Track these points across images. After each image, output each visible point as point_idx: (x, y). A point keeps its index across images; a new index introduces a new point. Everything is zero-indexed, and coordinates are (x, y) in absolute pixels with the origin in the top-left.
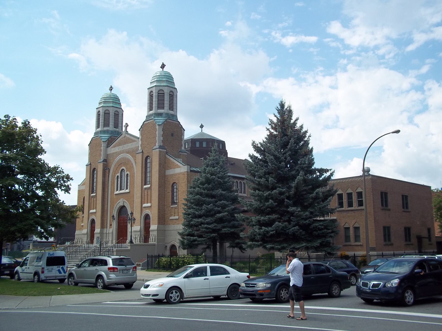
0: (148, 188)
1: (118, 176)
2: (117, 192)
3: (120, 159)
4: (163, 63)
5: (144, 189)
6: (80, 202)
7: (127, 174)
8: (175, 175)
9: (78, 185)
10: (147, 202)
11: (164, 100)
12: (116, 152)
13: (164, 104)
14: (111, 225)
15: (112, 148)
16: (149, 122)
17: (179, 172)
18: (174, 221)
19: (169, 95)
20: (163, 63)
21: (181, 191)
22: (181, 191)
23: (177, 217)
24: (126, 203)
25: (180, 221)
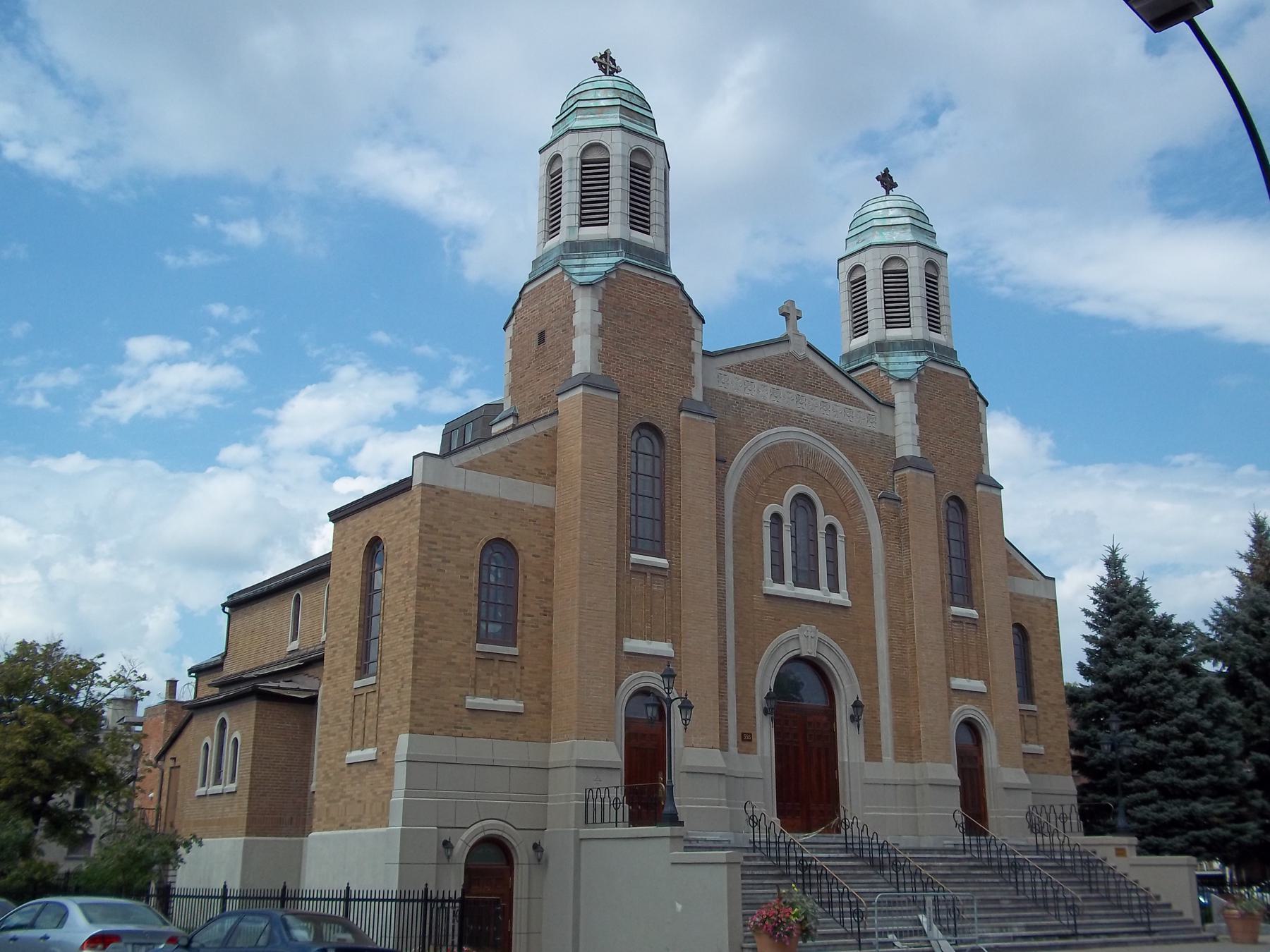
0: (968, 621)
1: (776, 517)
2: (778, 589)
4: (887, 170)
7: (831, 528)
11: (906, 304)
12: (762, 405)
13: (908, 319)
15: (728, 369)
19: (926, 297)
20: (887, 170)
21: (1041, 660)
22: (1041, 660)
23: (1040, 749)
24: (830, 648)
25: (1048, 763)
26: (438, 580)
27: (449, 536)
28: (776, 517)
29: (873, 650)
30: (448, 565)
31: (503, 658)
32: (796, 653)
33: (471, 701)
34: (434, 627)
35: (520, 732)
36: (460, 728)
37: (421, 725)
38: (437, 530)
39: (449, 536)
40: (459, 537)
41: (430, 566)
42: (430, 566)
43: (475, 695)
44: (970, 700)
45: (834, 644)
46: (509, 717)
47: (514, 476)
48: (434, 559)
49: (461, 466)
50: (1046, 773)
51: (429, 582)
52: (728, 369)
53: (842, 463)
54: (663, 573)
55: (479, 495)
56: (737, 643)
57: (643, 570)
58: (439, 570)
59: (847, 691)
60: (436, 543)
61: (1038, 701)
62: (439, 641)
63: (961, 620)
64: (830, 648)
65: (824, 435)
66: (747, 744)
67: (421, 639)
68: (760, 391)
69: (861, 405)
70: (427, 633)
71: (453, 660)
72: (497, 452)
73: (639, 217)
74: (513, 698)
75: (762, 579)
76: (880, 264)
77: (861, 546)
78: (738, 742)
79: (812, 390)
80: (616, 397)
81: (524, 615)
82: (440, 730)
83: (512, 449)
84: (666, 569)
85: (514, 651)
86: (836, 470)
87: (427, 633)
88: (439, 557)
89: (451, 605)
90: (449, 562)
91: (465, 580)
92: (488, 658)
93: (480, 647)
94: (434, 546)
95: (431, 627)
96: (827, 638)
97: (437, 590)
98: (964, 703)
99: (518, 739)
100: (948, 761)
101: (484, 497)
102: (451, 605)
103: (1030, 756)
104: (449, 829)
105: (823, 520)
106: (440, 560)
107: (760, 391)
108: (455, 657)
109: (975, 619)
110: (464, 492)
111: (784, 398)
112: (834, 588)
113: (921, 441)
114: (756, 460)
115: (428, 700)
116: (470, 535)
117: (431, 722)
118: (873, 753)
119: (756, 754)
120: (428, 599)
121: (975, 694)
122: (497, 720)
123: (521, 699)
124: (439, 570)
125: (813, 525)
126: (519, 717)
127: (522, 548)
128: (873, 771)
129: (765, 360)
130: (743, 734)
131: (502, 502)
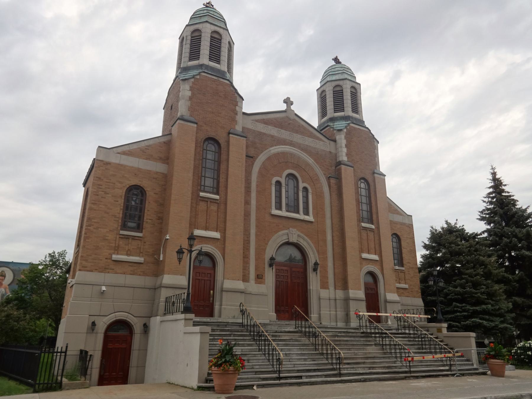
0: (370, 230)
1: (278, 183)
3: (284, 154)
4: (337, 57)
5: (362, 228)
6: (106, 193)
8: (394, 223)
9: (99, 147)
10: (375, 252)
12: (272, 136)
14: (260, 278)
16: (360, 129)
17: (402, 222)
18: (399, 290)
21: (406, 249)
22: (406, 249)
23: (406, 286)
26: (101, 202)
27: (109, 182)
28: (278, 183)
29: (325, 241)
30: (108, 195)
31: (134, 237)
32: (287, 240)
33: (115, 257)
34: (98, 223)
35: (141, 272)
36: (108, 269)
37: (86, 267)
38: (103, 180)
39: (109, 182)
40: (115, 184)
41: (98, 195)
42: (98, 195)
43: (118, 254)
44: (371, 263)
45: (306, 238)
46: (135, 265)
47: (147, 159)
48: (100, 192)
49: (118, 153)
50: (409, 297)
51: (96, 202)
52: (257, 121)
53: (311, 162)
54: (217, 201)
55: (127, 166)
56: (257, 235)
57: (206, 200)
58: (102, 197)
59: (312, 258)
60: (101, 185)
61: (405, 266)
62: (100, 229)
63: (367, 229)
64: (304, 239)
65: (302, 150)
66: (260, 280)
67: (89, 228)
68: (273, 131)
69: (321, 140)
70: (93, 225)
71: (107, 238)
72: (139, 148)
73: (215, 55)
74: (139, 256)
75: (271, 208)
76: (331, 88)
77: (319, 196)
78: (255, 279)
79: (297, 132)
80: (196, 125)
81: (147, 219)
82: (96, 270)
83: (147, 147)
84: (218, 200)
85: (140, 235)
86: (308, 164)
87: (93, 225)
88: (103, 191)
89: (108, 213)
90: (108, 194)
91: (117, 203)
92: (127, 237)
93: (122, 232)
94: (101, 187)
95: (95, 222)
96: (302, 235)
97: (100, 206)
98: (368, 265)
99: (140, 275)
100: (360, 290)
101: (130, 167)
102: (108, 213)
103: (401, 289)
104: (96, 316)
105: (301, 185)
106: (103, 193)
107: (273, 131)
108: (108, 236)
109: (373, 229)
110: (119, 164)
111: (284, 134)
112: (307, 213)
113: (347, 155)
114: (269, 159)
115: (91, 256)
116: (121, 183)
117: (91, 266)
118: (324, 285)
119: (265, 284)
120: (95, 210)
121: (373, 261)
122: (129, 266)
123: (142, 256)
124: (102, 197)
125: (297, 187)
126: (141, 265)
127: (148, 190)
128: (324, 293)
129: (275, 119)
130: (258, 275)
131: (139, 170)
